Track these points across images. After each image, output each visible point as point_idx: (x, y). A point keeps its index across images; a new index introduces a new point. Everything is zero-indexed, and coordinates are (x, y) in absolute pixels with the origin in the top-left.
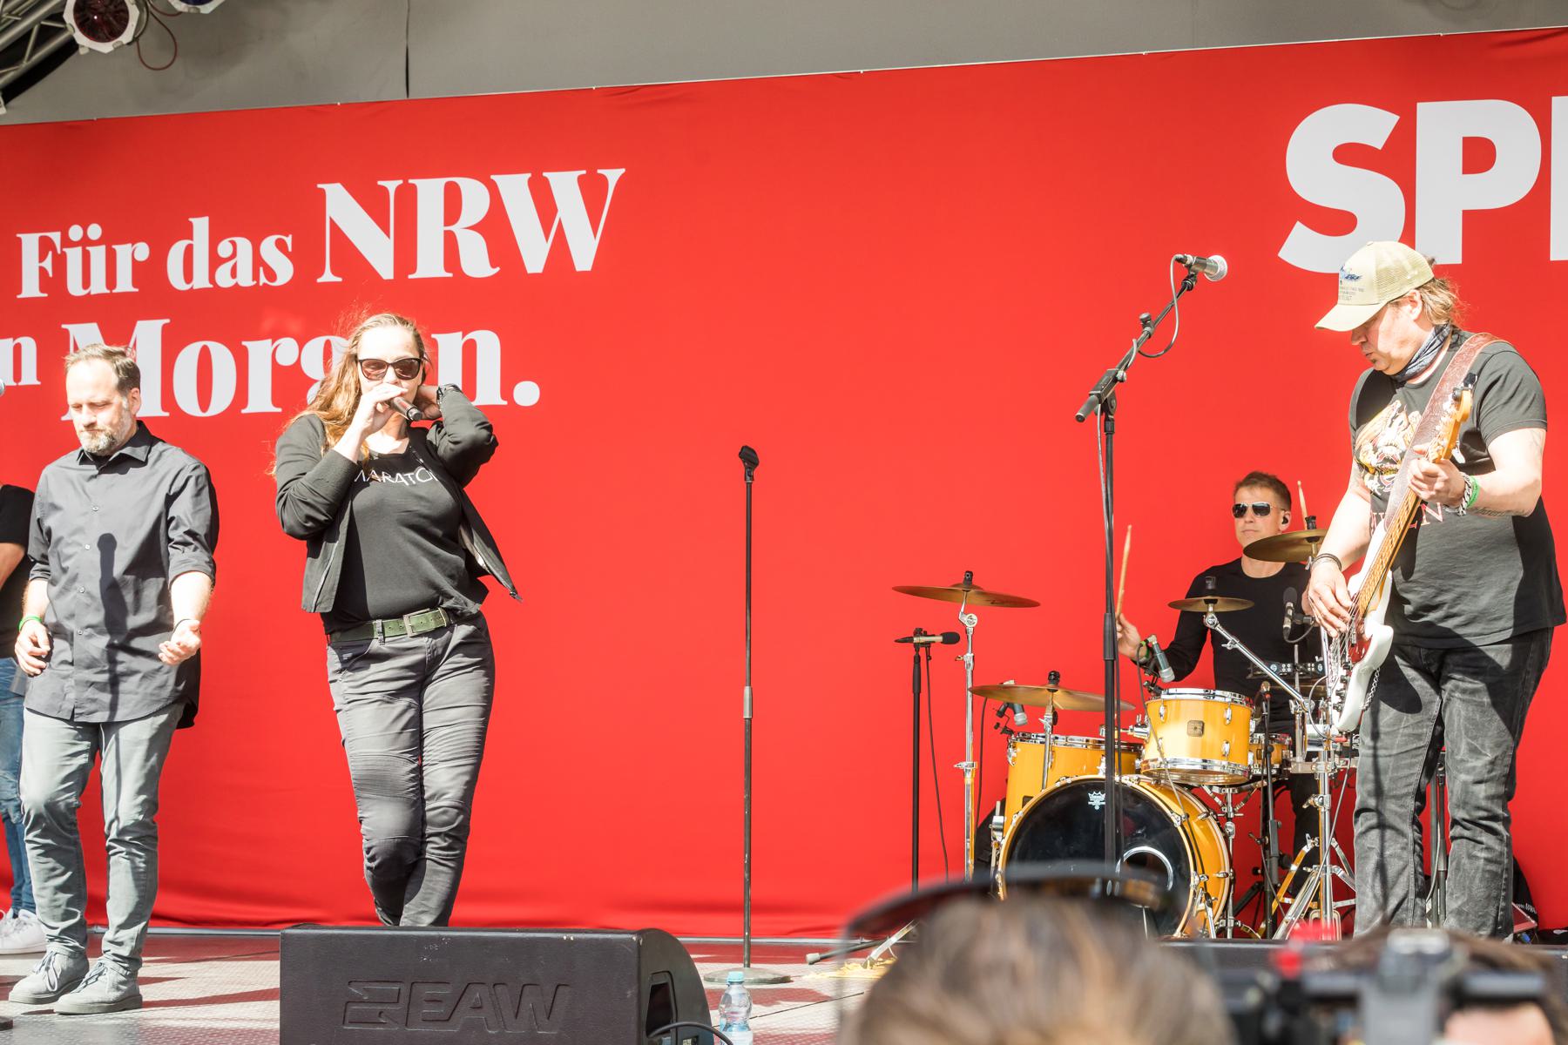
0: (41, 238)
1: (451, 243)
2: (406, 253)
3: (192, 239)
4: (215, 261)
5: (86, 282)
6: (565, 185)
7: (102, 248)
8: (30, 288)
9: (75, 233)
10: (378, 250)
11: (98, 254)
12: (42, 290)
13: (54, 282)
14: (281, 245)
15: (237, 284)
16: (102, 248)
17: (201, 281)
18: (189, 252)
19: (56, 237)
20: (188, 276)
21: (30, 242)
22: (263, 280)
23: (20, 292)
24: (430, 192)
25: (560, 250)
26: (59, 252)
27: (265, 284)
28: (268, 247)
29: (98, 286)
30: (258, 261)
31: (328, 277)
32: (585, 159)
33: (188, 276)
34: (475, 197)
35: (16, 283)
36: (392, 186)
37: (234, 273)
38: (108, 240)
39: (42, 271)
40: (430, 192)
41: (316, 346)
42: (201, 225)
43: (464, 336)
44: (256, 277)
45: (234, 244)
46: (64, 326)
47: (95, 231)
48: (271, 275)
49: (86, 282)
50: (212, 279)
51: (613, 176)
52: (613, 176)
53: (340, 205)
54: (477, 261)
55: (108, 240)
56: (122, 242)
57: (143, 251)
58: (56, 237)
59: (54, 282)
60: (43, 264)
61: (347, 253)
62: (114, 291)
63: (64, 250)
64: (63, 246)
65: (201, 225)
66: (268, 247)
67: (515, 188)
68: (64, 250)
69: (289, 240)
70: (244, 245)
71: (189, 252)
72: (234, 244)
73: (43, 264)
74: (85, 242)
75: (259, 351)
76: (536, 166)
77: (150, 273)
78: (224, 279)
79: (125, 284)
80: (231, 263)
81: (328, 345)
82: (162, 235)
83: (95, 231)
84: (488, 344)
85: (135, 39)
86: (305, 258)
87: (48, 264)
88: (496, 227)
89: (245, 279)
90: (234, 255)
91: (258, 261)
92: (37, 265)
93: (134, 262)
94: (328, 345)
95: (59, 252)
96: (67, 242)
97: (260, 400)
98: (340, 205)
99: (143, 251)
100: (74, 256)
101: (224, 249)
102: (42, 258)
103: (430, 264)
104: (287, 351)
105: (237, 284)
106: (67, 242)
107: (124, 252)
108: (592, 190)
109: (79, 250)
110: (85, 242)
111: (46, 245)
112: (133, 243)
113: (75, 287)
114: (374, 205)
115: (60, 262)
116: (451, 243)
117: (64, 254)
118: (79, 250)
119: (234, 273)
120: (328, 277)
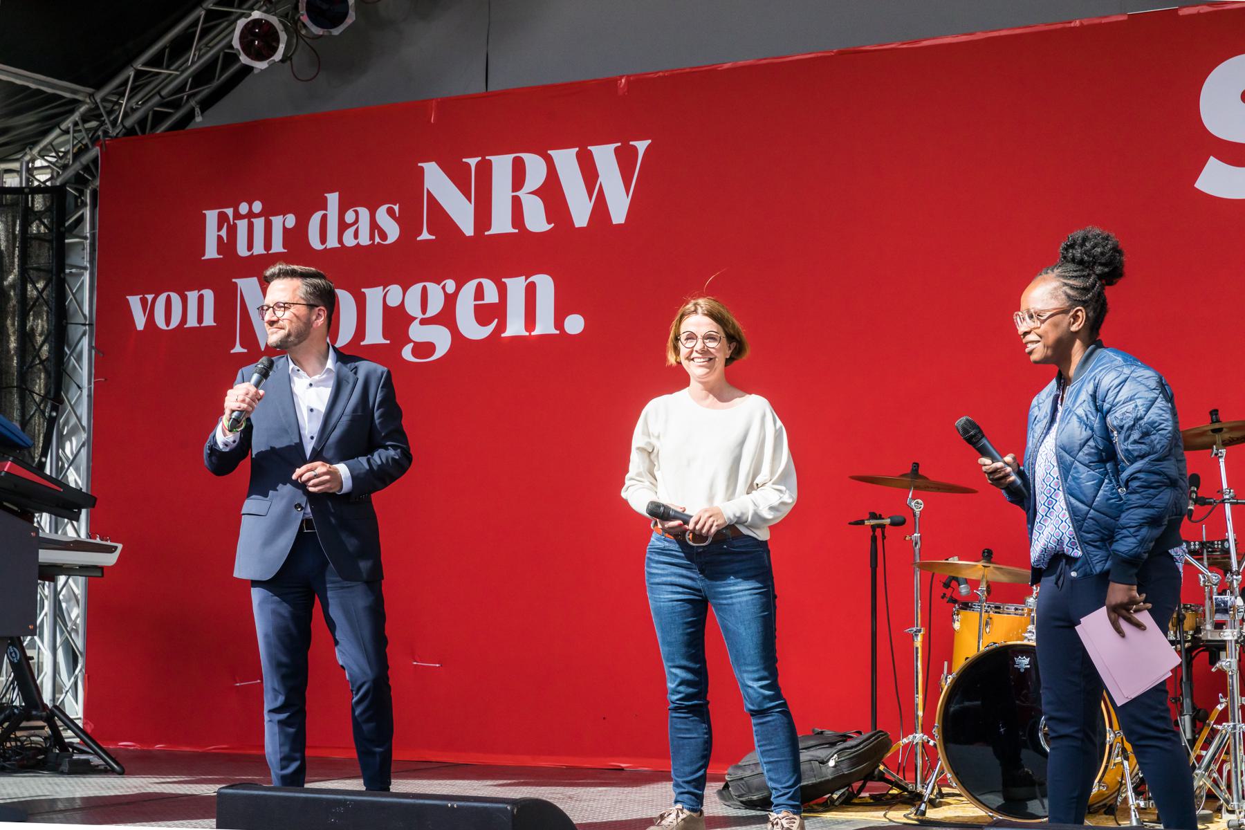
0: (219, 213)
1: (517, 204)
2: (483, 215)
3: (326, 210)
4: (343, 226)
5: (250, 246)
6: (605, 155)
7: (262, 219)
8: (211, 252)
9: (244, 208)
10: (462, 213)
11: (259, 223)
13: (227, 246)
14: (390, 212)
15: (358, 243)
16: (262, 219)
17: (332, 242)
18: (324, 219)
19: (230, 212)
20: (323, 239)
21: (211, 216)
22: (377, 240)
23: (204, 255)
24: (502, 165)
25: (600, 209)
26: (232, 223)
27: (378, 243)
28: (382, 214)
30: (374, 225)
31: (425, 235)
32: (620, 134)
33: (323, 239)
34: (536, 169)
36: (473, 162)
37: (356, 236)
38: (267, 213)
39: (220, 238)
40: (502, 165)
41: (416, 289)
42: (333, 199)
43: (526, 280)
44: (372, 237)
45: (356, 212)
46: (234, 280)
47: (257, 207)
48: (384, 236)
49: (250, 247)
50: (340, 240)
51: (642, 146)
52: (642, 146)
53: (435, 179)
54: (537, 220)
55: (267, 213)
57: (291, 221)
58: (230, 212)
59: (227, 246)
60: (220, 233)
61: (440, 218)
62: (270, 252)
63: (236, 221)
64: (234, 219)
65: (333, 199)
66: (382, 214)
67: (566, 159)
68: (236, 221)
69: (396, 208)
70: (364, 212)
71: (324, 219)
72: (356, 212)
73: (220, 233)
74: (251, 215)
75: (374, 296)
76: (583, 143)
77: (295, 237)
78: (349, 240)
79: (278, 246)
80: (354, 228)
81: (424, 291)
82: (307, 205)
83: (257, 207)
84: (545, 285)
85: (282, 61)
86: (409, 224)
87: (224, 233)
88: (551, 192)
89: (364, 240)
90: (356, 221)
91: (374, 225)
92: (215, 233)
93: (284, 228)
94: (424, 291)
95: (232, 223)
96: (238, 216)
97: (375, 335)
98: (435, 179)
99: (291, 221)
100: (242, 225)
101: (350, 217)
102: (220, 229)
103: (501, 223)
104: (395, 294)
105: (358, 243)
106: (238, 216)
107: (277, 221)
108: (625, 159)
109: (246, 221)
110: (251, 215)
111: (222, 218)
113: (242, 251)
114: (459, 177)
115: (232, 231)
116: (517, 204)
117: (235, 225)
118: (246, 221)
119: (356, 236)
120: (425, 235)
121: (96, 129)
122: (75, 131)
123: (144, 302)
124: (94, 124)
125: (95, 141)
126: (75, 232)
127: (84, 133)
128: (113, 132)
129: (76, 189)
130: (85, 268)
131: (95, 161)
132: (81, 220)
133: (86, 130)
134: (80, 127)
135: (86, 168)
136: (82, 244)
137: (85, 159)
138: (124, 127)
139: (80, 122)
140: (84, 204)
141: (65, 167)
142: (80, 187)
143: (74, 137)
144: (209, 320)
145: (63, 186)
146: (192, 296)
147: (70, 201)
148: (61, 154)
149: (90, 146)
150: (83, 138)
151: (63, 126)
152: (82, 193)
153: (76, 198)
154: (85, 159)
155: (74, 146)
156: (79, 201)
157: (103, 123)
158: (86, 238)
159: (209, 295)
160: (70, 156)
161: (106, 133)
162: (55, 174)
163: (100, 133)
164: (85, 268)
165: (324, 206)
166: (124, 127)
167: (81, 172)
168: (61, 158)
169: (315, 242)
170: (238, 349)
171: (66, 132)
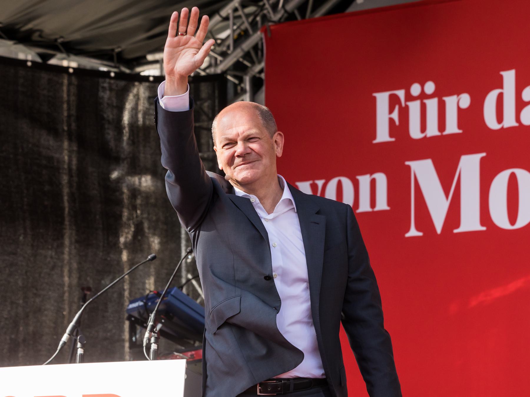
9: (415, 89)
11: (432, 105)
12: (391, 136)
17: (509, 121)
18: (500, 99)
19: (401, 94)
20: (500, 118)
23: (375, 138)
29: (432, 130)
33: (500, 118)
35: (373, 132)
38: (439, 94)
39: (391, 121)
47: (430, 87)
55: (439, 94)
57: (465, 100)
58: (401, 94)
71: (500, 99)
74: (423, 96)
83: (430, 87)
87: (395, 115)
93: (459, 109)
96: (409, 97)
99: (465, 100)
100: (414, 107)
102: (391, 111)
106: (409, 97)
107: (451, 102)
110: (423, 96)
111: (394, 101)
112: (458, 94)
113: (415, 133)
115: (404, 113)
117: (407, 107)
121: (255, 14)
122: (236, 18)
124: (251, 9)
125: (254, 24)
127: (244, 19)
128: (276, 17)
129: (235, 77)
131: (256, 48)
133: (247, 16)
134: (240, 13)
135: (247, 55)
137: (247, 45)
138: (286, 11)
139: (240, 8)
140: (244, 91)
141: (224, 55)
142: (238, 74)
143: (234, 24)
144: (382, 204)
145: (224, 73)
146: (364, 180)
147: (230, 91)
148: (219, 41)
149: (251, 31)
150: (243, 23)
151: (224, 13)
152: (241, 80)
153: (235, 86)
154: (247, 45)
155: (234, 31)
156: (239, 88)
157: (262, 8)
159: (381, 179)
160: (230, 42)
161: (265, 18)
162: (213, 62)
163: (258, 19)
165: (500, 86)
166: (286, 11)
167: (241, 60)
168: (219, 45)
169: (491, 122)
170: (413, 232)
171: (226, 19)
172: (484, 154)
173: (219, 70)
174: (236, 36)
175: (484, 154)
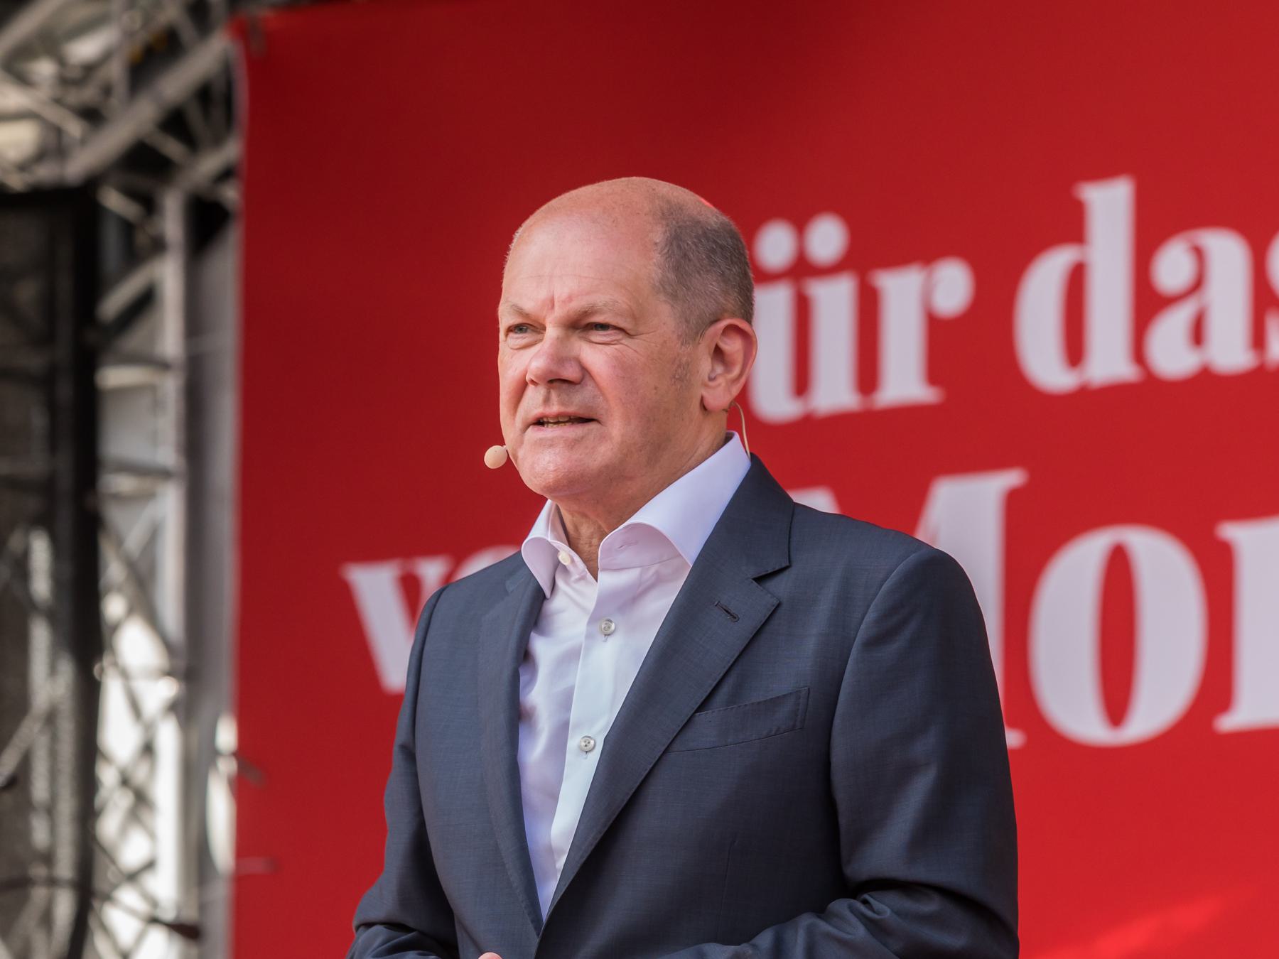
5: (802, 381)
18: (1076, 282)
20: (1075, 349)
33: (1075, 349)
37: (1198, 334)
45: (1199, 254)
49: (802, 381)
50: (1139, 354)
56: (897, 259)
71: (1076, 282)
72: (1199, 254)
90: (1198, 284)
119: (1198, 334)
123: (410, 586)
126: (133, 341)
129: (131, 194)
130: (164, 474)
132: (146, 301)
136: (152, 389)
140: (158, 246)
141: (93, 116)
142: (142, 182)
149: (187, 32)
152: (149, 205)
153: (128, 228)
156: (141, 239)
158: (163, 366)
160: (116, 71)
164: (164, 474)
172: (1011, 478)
173: (77, 167)
174: (137, 46)
175: (1011, 478)
